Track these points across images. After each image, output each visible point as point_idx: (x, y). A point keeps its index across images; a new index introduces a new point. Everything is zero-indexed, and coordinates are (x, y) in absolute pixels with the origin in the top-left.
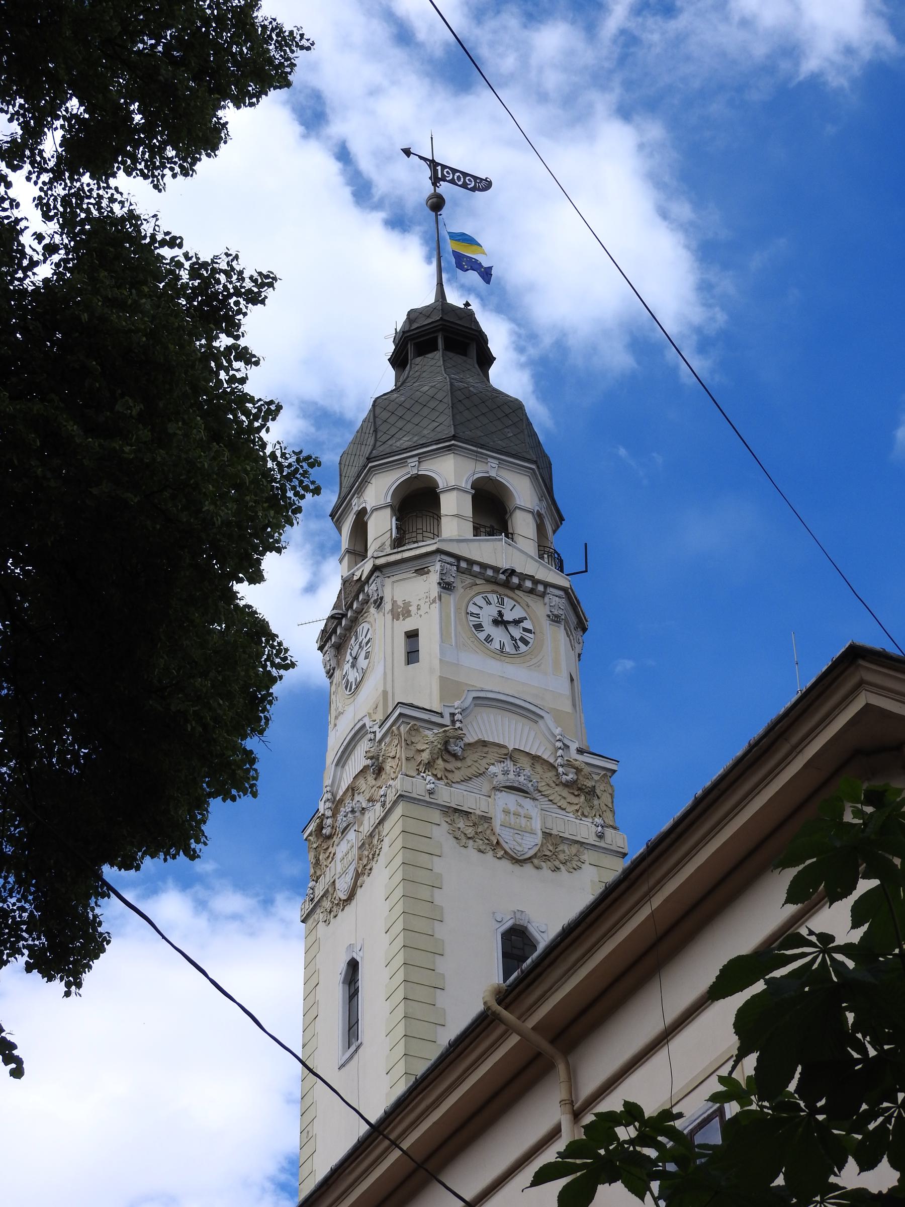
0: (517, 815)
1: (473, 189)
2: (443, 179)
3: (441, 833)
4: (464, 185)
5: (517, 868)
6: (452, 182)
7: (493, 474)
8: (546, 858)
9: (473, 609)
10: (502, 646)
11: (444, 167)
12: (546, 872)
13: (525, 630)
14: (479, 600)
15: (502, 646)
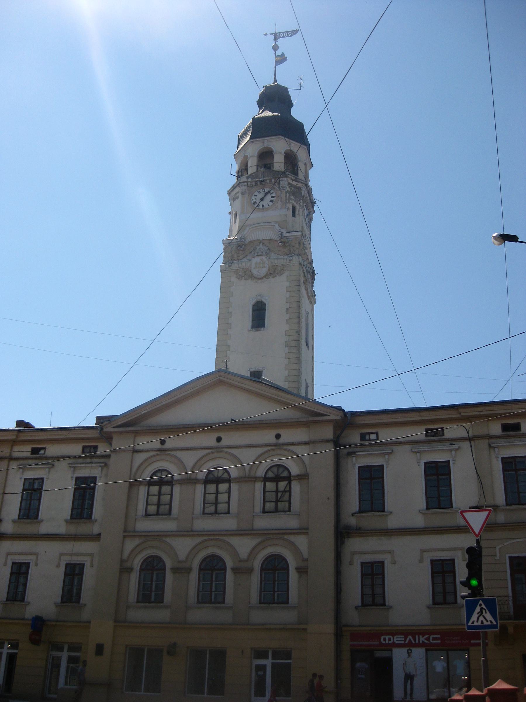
0: (260, 263)
1: (291, 36)
2: (280, 37)
3: (234, 279)
4: (288, 36)
5: (260, 281)
6: (283, 37)
7: (266, 146)
8: (271, 274)
9: (253, 198)
10: (263, 206)
11: (279, 33)
12: (272, 280)
13: (272, 197)
14: (256, 193)
15: (263, 206)
